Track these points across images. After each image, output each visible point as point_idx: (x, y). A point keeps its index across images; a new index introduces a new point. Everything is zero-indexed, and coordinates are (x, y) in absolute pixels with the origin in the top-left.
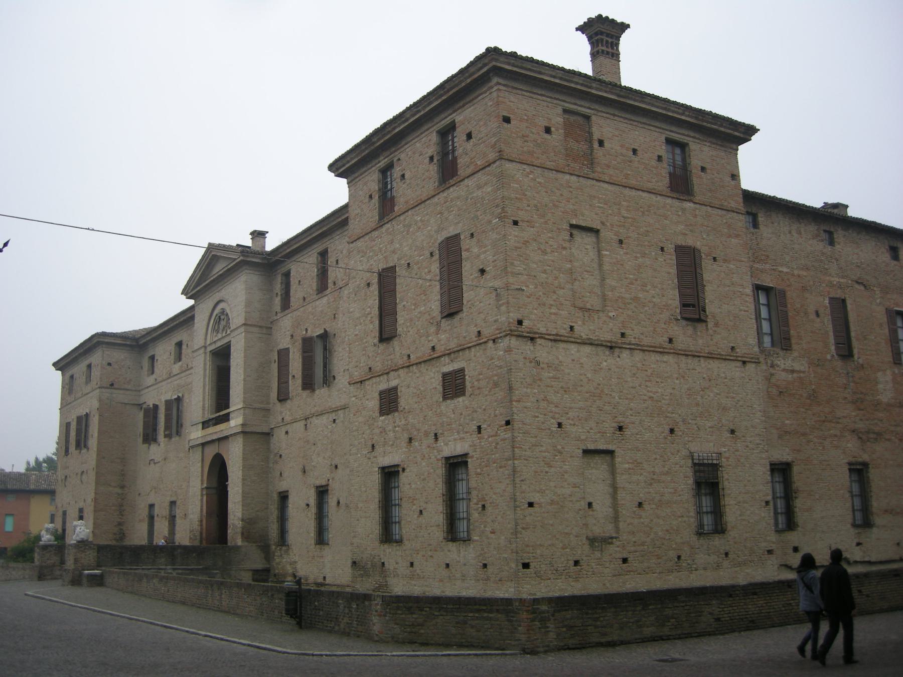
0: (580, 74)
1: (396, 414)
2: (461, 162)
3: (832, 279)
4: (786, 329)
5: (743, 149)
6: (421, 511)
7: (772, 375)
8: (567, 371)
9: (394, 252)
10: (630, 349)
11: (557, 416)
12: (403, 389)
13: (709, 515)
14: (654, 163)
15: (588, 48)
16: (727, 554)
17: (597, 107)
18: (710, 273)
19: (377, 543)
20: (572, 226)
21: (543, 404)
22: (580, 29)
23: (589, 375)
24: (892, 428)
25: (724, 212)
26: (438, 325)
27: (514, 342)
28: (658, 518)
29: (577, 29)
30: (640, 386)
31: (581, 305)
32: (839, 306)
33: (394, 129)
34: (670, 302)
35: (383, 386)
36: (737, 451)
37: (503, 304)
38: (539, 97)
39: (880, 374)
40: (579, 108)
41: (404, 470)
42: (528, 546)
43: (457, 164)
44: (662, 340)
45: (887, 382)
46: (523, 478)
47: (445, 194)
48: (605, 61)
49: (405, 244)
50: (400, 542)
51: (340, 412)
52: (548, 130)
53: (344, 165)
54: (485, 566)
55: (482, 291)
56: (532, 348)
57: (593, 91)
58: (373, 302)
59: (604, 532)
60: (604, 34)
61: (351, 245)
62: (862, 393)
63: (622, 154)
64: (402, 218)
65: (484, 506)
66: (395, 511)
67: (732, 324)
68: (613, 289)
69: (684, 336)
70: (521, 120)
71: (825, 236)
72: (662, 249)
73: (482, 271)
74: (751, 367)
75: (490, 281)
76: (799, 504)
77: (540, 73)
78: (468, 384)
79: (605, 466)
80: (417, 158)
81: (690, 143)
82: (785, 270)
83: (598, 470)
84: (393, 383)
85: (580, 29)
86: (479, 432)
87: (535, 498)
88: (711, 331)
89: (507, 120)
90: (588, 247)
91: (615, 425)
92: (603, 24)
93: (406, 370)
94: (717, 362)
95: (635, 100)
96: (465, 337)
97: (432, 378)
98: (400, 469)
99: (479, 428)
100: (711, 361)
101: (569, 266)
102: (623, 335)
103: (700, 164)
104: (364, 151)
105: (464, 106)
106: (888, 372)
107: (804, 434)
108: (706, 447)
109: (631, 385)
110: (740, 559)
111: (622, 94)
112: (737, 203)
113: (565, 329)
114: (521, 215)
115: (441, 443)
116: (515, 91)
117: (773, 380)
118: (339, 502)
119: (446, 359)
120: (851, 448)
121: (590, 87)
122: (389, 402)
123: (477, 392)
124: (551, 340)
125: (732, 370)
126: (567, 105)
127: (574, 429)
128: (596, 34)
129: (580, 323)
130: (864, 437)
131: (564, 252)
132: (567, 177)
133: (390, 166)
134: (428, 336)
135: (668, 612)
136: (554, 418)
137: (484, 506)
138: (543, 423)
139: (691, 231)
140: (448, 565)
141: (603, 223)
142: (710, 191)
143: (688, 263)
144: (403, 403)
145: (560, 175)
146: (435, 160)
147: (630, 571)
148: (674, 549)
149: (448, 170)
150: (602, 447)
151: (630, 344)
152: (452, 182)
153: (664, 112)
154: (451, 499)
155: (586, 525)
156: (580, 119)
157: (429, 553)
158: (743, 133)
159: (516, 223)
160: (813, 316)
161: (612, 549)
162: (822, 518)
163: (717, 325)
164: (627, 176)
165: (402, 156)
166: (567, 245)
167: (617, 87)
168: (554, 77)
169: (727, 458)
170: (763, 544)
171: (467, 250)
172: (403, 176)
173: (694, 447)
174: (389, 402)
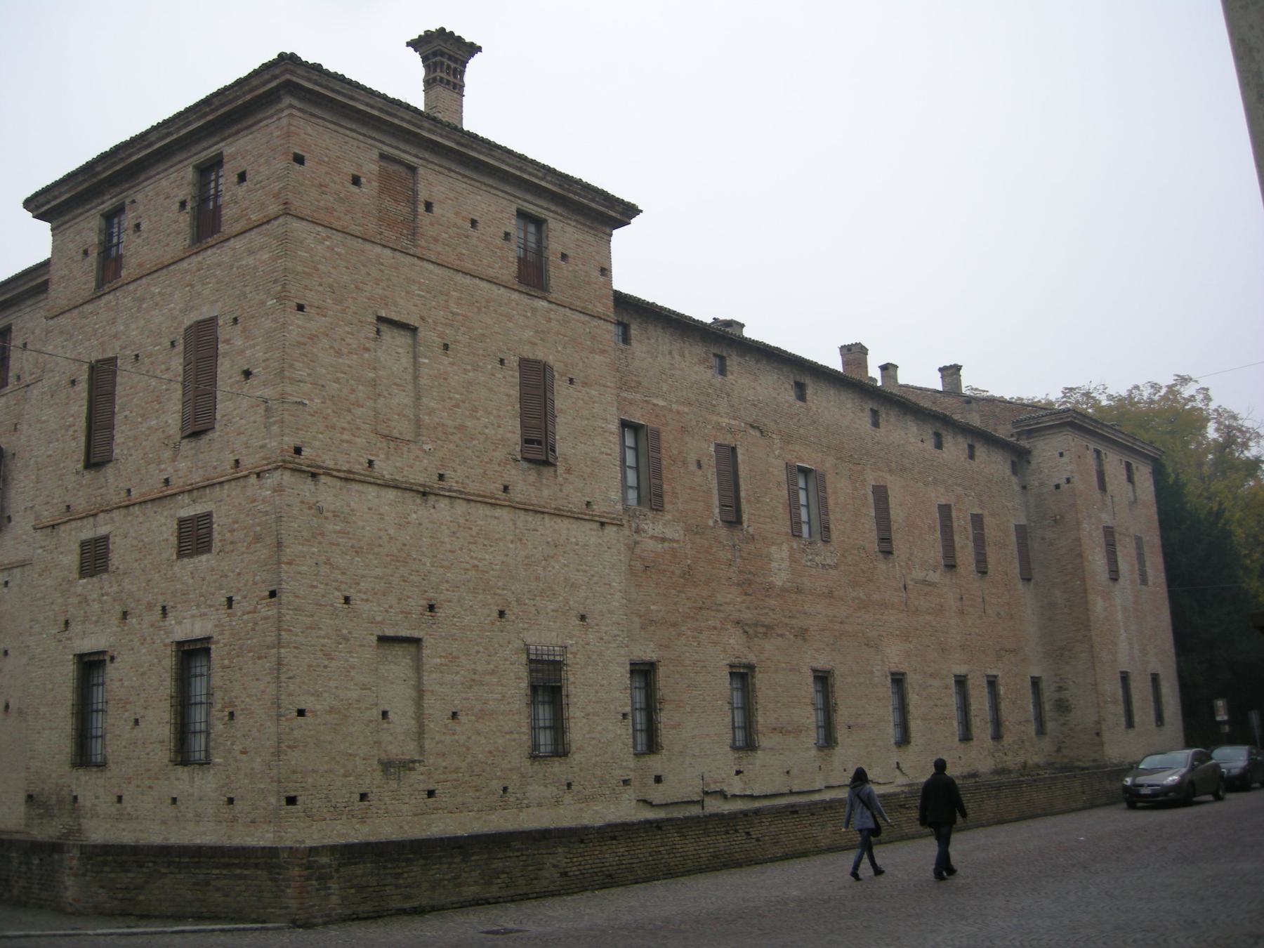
0: (407, 107)
1: (105, 576)
2: (227, 213)
3: (721, 420)
4: (657, 482)
5: (619, 236)
6: (137, 722)
7: (637, 543)
8: (361, 523)
9: (115, 336)
10: (450, 497)
11: (343, 587)
12: (117, 539)
13: (548, 731)
14: (499, 242)
15: (421, 72)
16: (569, 785)
17: (427, 155)
18: (564, 399)
19: (67, 768)
20: (380, 319)
21: (324, 569)
22: (413, 44)
23: (391, 531)
24: (787, 621)
25: (587, 318)
26: (176, 448)
27: (287, 477)
28: (479, 734)
29: (409, 44)
30: (461, 549)
31: (386, 432)
32: (728, 456)
33: (130, 155)
34: (509, 435)
35: (87, 534)
36: (588, 644)
37: (275, 422)
38: (348, 132)
39: (773, 549)
40: (403, 155)
41: (112, 659)
42: (294, 772)
43: (220, 216)
44: (495, 487)
45: (782, 559)
46: (290, 674)
47: (200, 258)
48: (443, 93)
49: (133, 326)
50: (102, 765)
51: (15, 571)
52: (356, 181)
53: (48, 203)
55: (245, 403)
56: (313, 488)
57: (424, 133)
58: (79, 408)
59: (403, 754)
60: (445, 55)
61: (51, 322)
62: (750, 572)
63: (456, 225)
64: (131, 287)
65: (232, 715)
66: (98, 721)
67: (589, 470)
68: (431, 412)
69: (524, 483)
70: (320, 162)
71: (714, 362)
72: (502, 361)
73: (247, 374)
74: (611, 530)
75: (257, 389)
76: (665, 718)
77: (352, 98)
78: (216, 535)
79: (408, 661)
80: (162, 201)
81: (550, 220)
82: (661, 403)
83: (398, 665)
84: (102, 531)
85: (413, 44)
86: (230, 607)
87: (308, 703)
88: (560, 479)
89: (299, 160)
90: (400, 350)
91: (424, 603)
92: (445, 41)
93: (123, 511)
94: (566, 521)
95: (480, 153)
96: (215, 468)
97: (161, 527)
98: (107, 658)
99: (230, 600)
100: (558, 520)
101: (372, 375)
102: (441, 477)
103: (560, 249)
104: (81, 183)
105: (237, 132)
106: (785, 547)
107: (674, 625)
108: (546, 638)
109: (449, 547)
110: (586, 793)
111: (463, 141)
112: (606, 307)
113: (361, 464)
114: (310, 298)
115: (171, 621)
116: (314, 120)
117: (638, 551)
118: (7, 707)
119: (186, 499)
120: (734, 645)
121: (420, 127)
122: (95, 558)
123: (229, 548)
124: (341, 478)
125: (586, 534)
126: (385, 148)
127: (366, 606)
128: (435, 54)
129: (382, 456)
130: (751, 631)
131: (366, 355)
132: (378, 249)
133: (119, 210)
134: (159, 464)
135: (498, 864)
136: (338, 589)
137: (232, 715)
138: (323, 596)
139: (542, 340)
140: (174, 800)
141: (423, 319)
142: (572, 287)
143: (536, 383)
144: (115, 560)
145: (368, 246)
146: (188, 208)
147: (437, 809)
148: (499, 778)
149: (206, 223)
150: (404, 633)
151: (450, 491)
152: (211, 241)
153: (518, 173)
154: (183, 703)
155: (378, 743)
156: (402, 170)
157: (148, 783)
158: (621, 214)
159: (301, 308)
160: (693, 467)
161: (414, 777)
162: (694, 737)
163: (569, 471)
164: (460, 257)
165: (139, 197)
166: (371, 345)
167: (456, 130)
168: (372, 107)
169: (575, 654)
170: (619, 772)
171: (227, 341)
172: (138, 226)
173: (530, 637)
174: (95, 558)
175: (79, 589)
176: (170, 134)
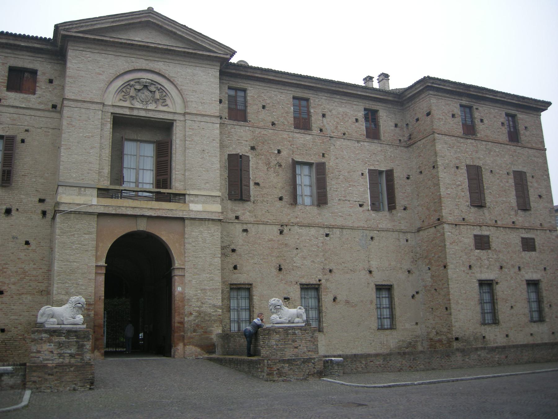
1: (489, 251)
12: (494, 238)
33: (486, 94)
53: (439, 85)
54: (553, 333)
65: (550, 306)
93: (495, 228)
105: (523, 112)
115: (523, 272)
118: (335, 299)
123: (542, 251)
140: (531, 334)
157: (520, 329)
175: (476, 254)
176: (505, 98)
